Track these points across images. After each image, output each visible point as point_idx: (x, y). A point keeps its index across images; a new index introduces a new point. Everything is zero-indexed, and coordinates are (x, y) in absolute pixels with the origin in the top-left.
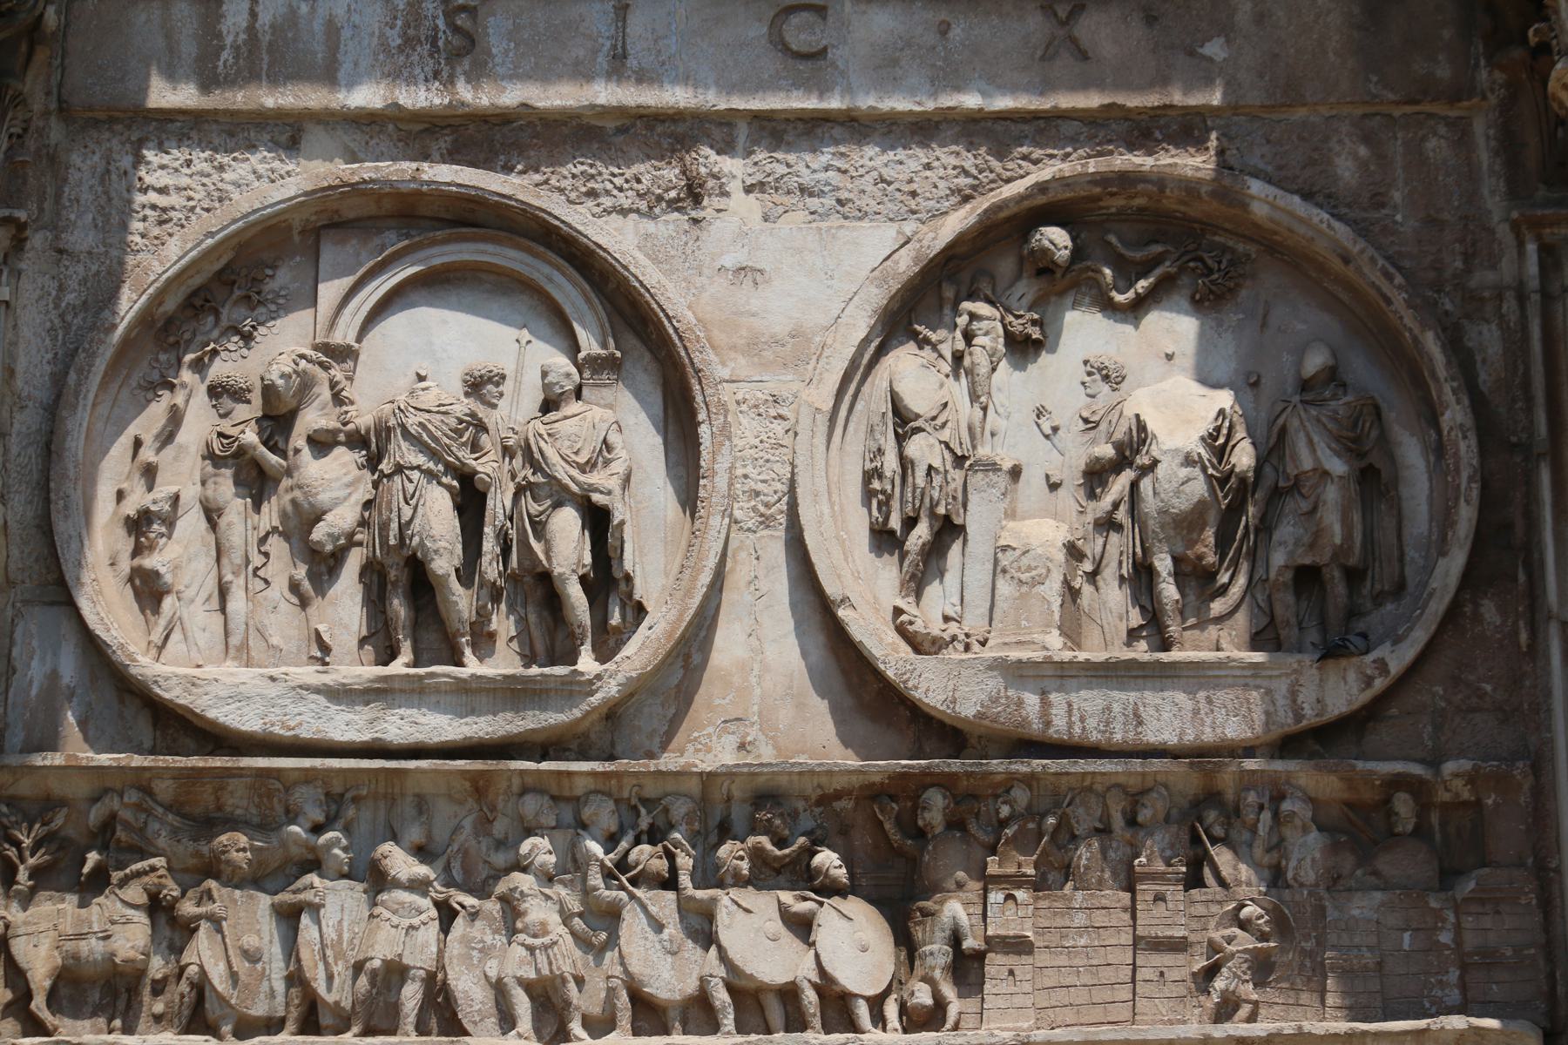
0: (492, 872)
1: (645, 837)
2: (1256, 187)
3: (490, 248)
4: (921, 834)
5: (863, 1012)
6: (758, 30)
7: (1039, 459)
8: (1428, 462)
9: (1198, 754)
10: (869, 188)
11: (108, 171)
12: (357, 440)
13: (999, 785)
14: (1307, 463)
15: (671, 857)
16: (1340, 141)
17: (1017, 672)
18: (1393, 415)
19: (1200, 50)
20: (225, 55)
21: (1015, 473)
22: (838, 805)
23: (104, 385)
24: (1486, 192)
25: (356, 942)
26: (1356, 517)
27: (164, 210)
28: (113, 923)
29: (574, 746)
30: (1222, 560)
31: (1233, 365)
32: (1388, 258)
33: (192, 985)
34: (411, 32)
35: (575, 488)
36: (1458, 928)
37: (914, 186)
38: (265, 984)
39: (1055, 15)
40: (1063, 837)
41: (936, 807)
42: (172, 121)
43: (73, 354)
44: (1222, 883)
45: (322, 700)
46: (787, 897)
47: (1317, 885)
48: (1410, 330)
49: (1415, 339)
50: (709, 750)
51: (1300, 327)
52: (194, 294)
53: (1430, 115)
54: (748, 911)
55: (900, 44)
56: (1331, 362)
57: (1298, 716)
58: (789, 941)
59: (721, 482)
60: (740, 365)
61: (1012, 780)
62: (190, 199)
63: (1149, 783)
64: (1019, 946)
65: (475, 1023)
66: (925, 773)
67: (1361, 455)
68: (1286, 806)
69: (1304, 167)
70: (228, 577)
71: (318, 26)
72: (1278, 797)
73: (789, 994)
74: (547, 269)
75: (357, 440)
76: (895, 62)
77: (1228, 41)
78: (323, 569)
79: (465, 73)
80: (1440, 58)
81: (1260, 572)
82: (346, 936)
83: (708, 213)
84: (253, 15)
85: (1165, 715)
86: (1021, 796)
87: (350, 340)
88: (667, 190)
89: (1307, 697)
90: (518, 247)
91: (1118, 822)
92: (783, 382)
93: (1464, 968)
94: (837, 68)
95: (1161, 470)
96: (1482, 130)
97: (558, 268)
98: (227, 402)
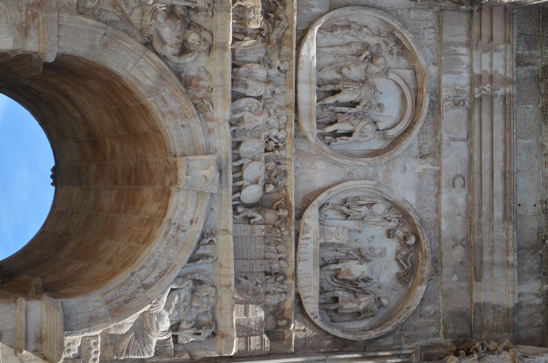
1: (277, 145)
2: (424, 287)
3: (410, 109)
4: (277, 209)
5: (237, 195)
6: (459, 172)
13: (289, 228)
15: (272, 151)
16: (434, 307)
20: (454, 48)
21: (359, 232)
22: (284, 190)
23: (380, 19)
24: (423, 341)
26: (350, 311)
29: (298, 128)
30: (340, 280)
32: (408, 318)
34: (459, 91)
39: (463, 241)
40: (277, 243)
41: (283, 213)
42: (439, 35)
43: (386, 12)
44: (266, 280)
46: (262, 178)
47: (266, 302)
49: (390, 325)
51: (392, 298)
52: (400, 41)
53: (440, 328)
55: (456, 205)
56: (385, 305)
57: (304, 298)
59: (358, 163)
61: (290, 231)
62: (422, 40)
63: (289, 263)
64: (252, 232)
66: (292, 211)
67: (363, 312)
68: (284, 295)
69: (428, 298)
71: (460, 70)
72: (286, 293)
76: (452, 204)
77: (457, 281)
78: (338, 70)
81: (337, 289)
82: (254, 74)
83: (418, 160)
84: (463, 55)
86: (286, 233)
89: (309, 300)
90: (411, 116)
91: (280, 256)
95: (360, 265)
96: (437, 340)
97: (406, 125)
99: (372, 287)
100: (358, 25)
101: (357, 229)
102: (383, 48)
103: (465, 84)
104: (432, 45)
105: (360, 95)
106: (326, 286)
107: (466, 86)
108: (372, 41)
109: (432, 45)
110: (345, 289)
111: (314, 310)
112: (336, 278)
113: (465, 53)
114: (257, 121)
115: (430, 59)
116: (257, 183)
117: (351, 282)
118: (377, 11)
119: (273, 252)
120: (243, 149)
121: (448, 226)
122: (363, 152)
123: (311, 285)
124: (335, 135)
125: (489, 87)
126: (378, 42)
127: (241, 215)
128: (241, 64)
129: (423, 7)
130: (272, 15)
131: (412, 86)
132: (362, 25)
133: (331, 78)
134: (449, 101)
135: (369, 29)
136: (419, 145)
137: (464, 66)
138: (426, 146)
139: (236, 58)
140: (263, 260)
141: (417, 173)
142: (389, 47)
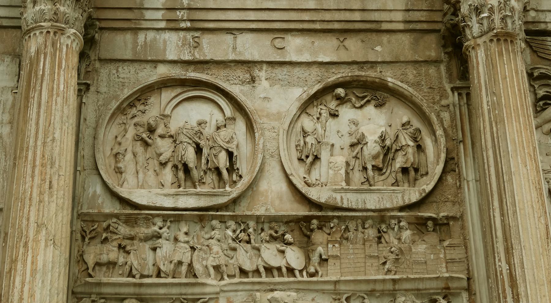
5: (297, 273)
6: (268, 43)
7: (338, 143)
9: (380, 211)
10: (296, 79)
12: (171, 136)
14: (404, 144)
15: (249, 236)
17: (335, 191)
18: (424, 133)
20: (139, 47)
21: (333, 145)
22: (290, 224)
25: (171, 256)
28: (109, 251)
30: (384, 165)
31: (385, 121)
35: (225, 147)
36: (445, 253)
37: (307, 79)
38: (147, 266)
44: (387, 242)
45: (162, 197)
46: (278, 246)
47: (410, 243)
50: (258, 210)
52: (131, 102)
54: (268, 249)
58: (279, 256)
60: (265, 120)
64: (336, 257)
67: (417, 141)
68: (402, 224)
70: (139, 168)
71: (161, 41)
73: (279, 269)
74: (217, 97)
75: (171, 136)
76: (301, 51)
80: (432, 51)
81: (393, 170)
83: (257, 85)
84: (146, 38)
85: (372, 202)
87: (169, 113)
92: (276, 124)
93: (447, 263)
95: (369, 144)
97: (220, 97)
98: (139, 128)
100: (114, 146)
102: (139, 120)
103: (176, 37)
104: (136, 69)
105: (189, 143)
106: (391, 180)
107: (179, 35)
108: (131, 132)
109: (136, 69)
111: (417, 193)
113: (144, 36)
115: (150, 71)
116: (283, 252)
117: (386, 155)
119: (357, 235)
120: (248, 267)
121: (325, 55)
122: (248, 142)
123: (391, 195)
124: (231, 169)
125: (180, 12)
126: (133, 125)
127: (318, 269)
128: (156, 269)
129: (96, 79)
130: (104, 235)
131: (179, 90)
132: (114, 141)
133: (171, 174)
134: (194, 52)
135: (119, 135)
137: (158, 37)
139: (150, 274)
140: (366, 246)
142: (138, 113)
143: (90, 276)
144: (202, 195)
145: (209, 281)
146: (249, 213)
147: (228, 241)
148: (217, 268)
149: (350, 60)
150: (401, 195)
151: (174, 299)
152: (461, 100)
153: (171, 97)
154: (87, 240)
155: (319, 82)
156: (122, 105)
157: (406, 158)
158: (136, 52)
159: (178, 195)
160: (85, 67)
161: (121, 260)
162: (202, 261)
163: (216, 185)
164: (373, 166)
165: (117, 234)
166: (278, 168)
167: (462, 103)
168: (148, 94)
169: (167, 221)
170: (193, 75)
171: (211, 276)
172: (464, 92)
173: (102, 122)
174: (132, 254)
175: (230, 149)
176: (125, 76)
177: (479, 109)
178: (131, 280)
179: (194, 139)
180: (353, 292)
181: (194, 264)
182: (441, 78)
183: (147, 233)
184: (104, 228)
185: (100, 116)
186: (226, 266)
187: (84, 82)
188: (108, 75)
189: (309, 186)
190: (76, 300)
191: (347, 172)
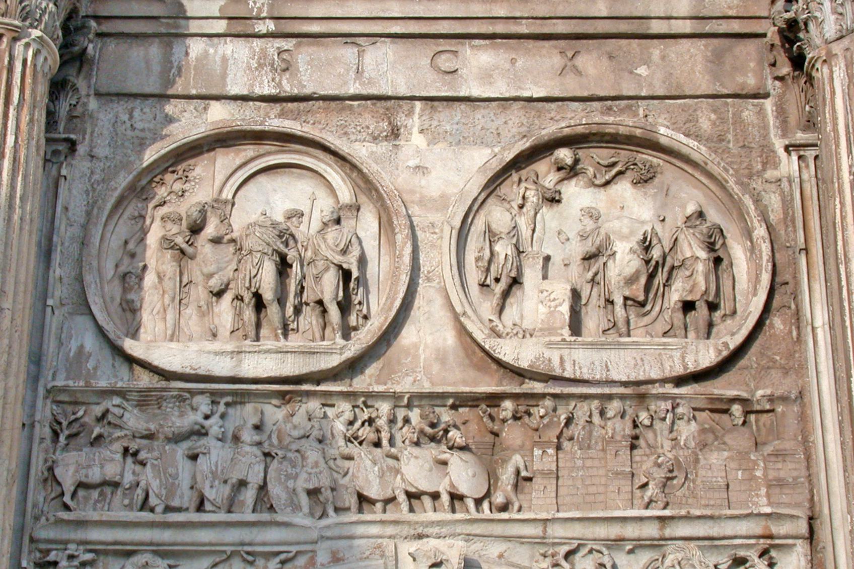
0: (292, 440)
3: (297, 156)
8: (746, 255)
9: (638, 383)
11: (116, 122)
14: (688, 255)
15: (378, 431)
19: (635, 71)
20: (173, 71)
21: (547, 259)
25: (225, 471)
27: (143, 139)
31: (652, 212)
33: (143, 490)
34: (262, 61)
35: (335, 262)
36: (765, 469)
44: (649, 446)
47: (696, 448)
48: (737, 194)
49: (740, 199)
50: (399, 383)
57: (686, 368)
62: (155, 134)
65: (282, 510)
68: (680, 410)
69: (685, 124)
73: (435, 496)
75: (233, 241)
77: (648, 67)
79: (287, 79)
81: (666, 305)
82: (220, 468)
83: (402, 143)
88: (381, 132)
92: (435, 217)
93: (769, 487)
94: (463, 78)
95: (618, 256)
97: (329, 165)
98: (169, 225)
99: (665, 234)
100: (122, 259)
101: (541, 264)
102: (171, 210)
106: (661, 326)
110: (666, 288)
111: (711, 350)
112: (642, 305)
114: (316, 464)
116: (445, 463)
117: (651, 277)
118: (95, 220)
119: (590, 433)
120: (372, 492)
121: (536, 84)
123: (660, 355)
128: (196, 494)
129: (89, 131)
130: (97, 431)
131: (249, 151)
132: (122, 251)
135: (131, 238)
136: (371, 139)
137: (212, 51)
138: (372, 127)
139: (185, 506)
141: (428, 145)
142: (169, 198)
143: (67, 507)
144: (288, 352)
145: (299, 519)
146: (381, 388)
147: (337, 442)
148: (313, 493)
149: (585, 94)
150: (678, 354)
151: (229, 553)
152: (804, 171)
153: (235, 167)
154: (62, 438)
155: (525, 136)
156: (140, 180)
157: (691, 283)
158: (169, 80)
159: (241, 352)
160: (67, 109)
161: (128, 479)
162: (286, 481)
163: (318, 336)
164: (626, 299)
165: (121, 428)
166: (439, 301)
167: (805, 176)
168: (192, 162)
169: (219, 403)
170: (275, 122)
171: (303, 510)
172: (810, 153)
173: (98, 214)
174: (148, 466)
175: (345, 266)
176: (146, 126)
177: (833, 182)
178: (146, 516)
179: (276, 245)
180: (580, 542)
181: (270, 486)
182: (765, 127)
183: (179, 427)
184: (96, 417)
185: (95, 202)
186: (333, 490)
187: (64, 136)
188: (114, 125)
189: (499, 336)
190: (38, 555)
191: (574, 310)
